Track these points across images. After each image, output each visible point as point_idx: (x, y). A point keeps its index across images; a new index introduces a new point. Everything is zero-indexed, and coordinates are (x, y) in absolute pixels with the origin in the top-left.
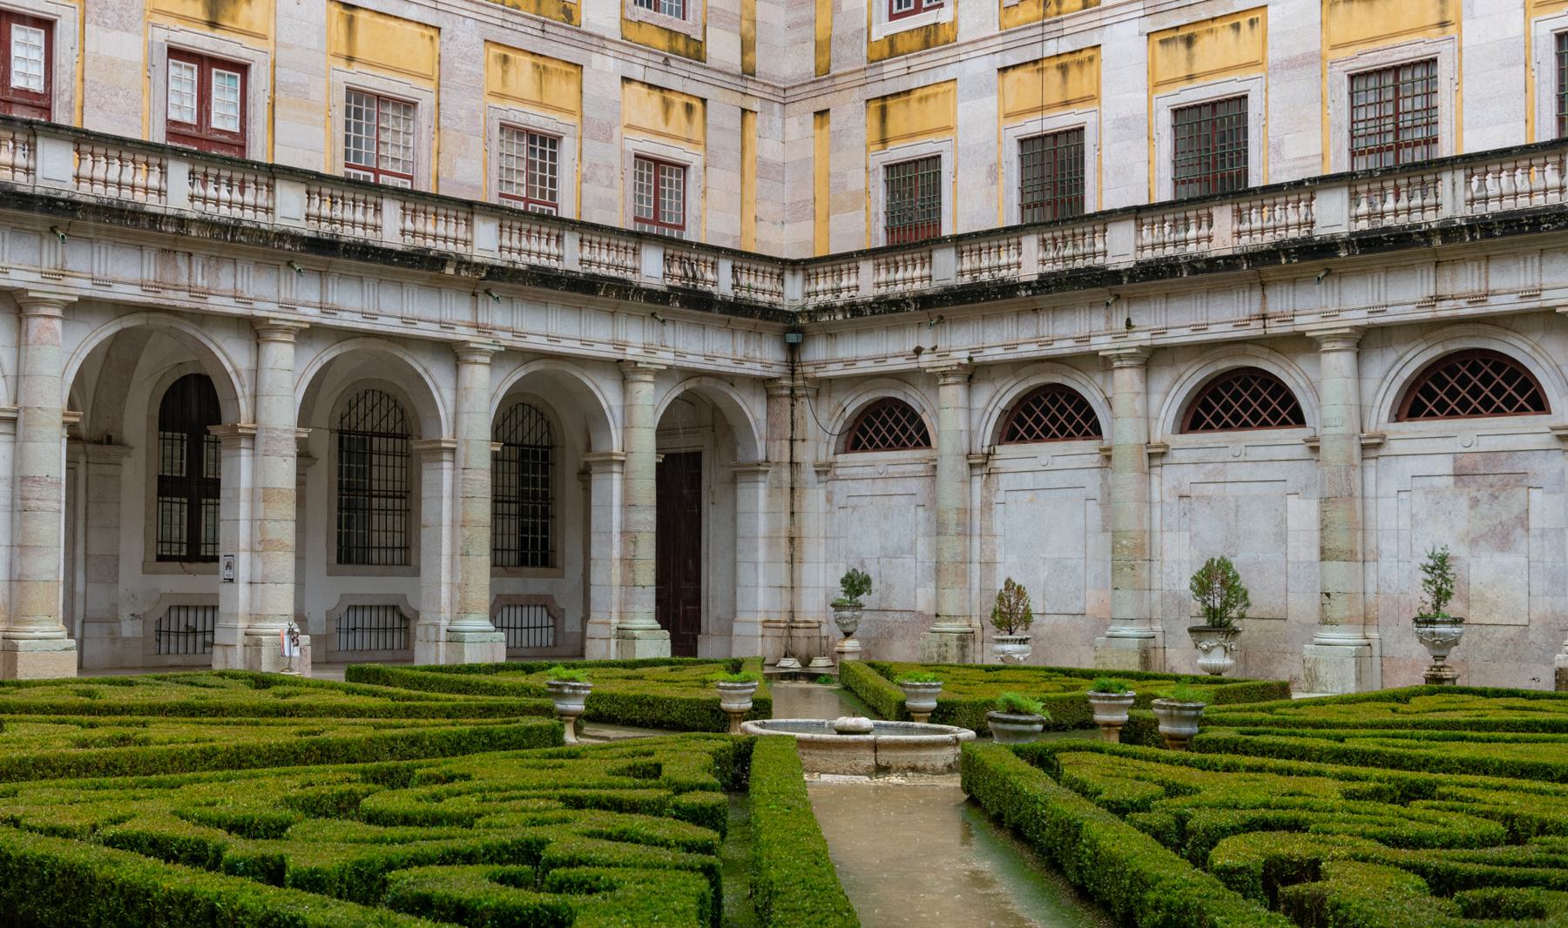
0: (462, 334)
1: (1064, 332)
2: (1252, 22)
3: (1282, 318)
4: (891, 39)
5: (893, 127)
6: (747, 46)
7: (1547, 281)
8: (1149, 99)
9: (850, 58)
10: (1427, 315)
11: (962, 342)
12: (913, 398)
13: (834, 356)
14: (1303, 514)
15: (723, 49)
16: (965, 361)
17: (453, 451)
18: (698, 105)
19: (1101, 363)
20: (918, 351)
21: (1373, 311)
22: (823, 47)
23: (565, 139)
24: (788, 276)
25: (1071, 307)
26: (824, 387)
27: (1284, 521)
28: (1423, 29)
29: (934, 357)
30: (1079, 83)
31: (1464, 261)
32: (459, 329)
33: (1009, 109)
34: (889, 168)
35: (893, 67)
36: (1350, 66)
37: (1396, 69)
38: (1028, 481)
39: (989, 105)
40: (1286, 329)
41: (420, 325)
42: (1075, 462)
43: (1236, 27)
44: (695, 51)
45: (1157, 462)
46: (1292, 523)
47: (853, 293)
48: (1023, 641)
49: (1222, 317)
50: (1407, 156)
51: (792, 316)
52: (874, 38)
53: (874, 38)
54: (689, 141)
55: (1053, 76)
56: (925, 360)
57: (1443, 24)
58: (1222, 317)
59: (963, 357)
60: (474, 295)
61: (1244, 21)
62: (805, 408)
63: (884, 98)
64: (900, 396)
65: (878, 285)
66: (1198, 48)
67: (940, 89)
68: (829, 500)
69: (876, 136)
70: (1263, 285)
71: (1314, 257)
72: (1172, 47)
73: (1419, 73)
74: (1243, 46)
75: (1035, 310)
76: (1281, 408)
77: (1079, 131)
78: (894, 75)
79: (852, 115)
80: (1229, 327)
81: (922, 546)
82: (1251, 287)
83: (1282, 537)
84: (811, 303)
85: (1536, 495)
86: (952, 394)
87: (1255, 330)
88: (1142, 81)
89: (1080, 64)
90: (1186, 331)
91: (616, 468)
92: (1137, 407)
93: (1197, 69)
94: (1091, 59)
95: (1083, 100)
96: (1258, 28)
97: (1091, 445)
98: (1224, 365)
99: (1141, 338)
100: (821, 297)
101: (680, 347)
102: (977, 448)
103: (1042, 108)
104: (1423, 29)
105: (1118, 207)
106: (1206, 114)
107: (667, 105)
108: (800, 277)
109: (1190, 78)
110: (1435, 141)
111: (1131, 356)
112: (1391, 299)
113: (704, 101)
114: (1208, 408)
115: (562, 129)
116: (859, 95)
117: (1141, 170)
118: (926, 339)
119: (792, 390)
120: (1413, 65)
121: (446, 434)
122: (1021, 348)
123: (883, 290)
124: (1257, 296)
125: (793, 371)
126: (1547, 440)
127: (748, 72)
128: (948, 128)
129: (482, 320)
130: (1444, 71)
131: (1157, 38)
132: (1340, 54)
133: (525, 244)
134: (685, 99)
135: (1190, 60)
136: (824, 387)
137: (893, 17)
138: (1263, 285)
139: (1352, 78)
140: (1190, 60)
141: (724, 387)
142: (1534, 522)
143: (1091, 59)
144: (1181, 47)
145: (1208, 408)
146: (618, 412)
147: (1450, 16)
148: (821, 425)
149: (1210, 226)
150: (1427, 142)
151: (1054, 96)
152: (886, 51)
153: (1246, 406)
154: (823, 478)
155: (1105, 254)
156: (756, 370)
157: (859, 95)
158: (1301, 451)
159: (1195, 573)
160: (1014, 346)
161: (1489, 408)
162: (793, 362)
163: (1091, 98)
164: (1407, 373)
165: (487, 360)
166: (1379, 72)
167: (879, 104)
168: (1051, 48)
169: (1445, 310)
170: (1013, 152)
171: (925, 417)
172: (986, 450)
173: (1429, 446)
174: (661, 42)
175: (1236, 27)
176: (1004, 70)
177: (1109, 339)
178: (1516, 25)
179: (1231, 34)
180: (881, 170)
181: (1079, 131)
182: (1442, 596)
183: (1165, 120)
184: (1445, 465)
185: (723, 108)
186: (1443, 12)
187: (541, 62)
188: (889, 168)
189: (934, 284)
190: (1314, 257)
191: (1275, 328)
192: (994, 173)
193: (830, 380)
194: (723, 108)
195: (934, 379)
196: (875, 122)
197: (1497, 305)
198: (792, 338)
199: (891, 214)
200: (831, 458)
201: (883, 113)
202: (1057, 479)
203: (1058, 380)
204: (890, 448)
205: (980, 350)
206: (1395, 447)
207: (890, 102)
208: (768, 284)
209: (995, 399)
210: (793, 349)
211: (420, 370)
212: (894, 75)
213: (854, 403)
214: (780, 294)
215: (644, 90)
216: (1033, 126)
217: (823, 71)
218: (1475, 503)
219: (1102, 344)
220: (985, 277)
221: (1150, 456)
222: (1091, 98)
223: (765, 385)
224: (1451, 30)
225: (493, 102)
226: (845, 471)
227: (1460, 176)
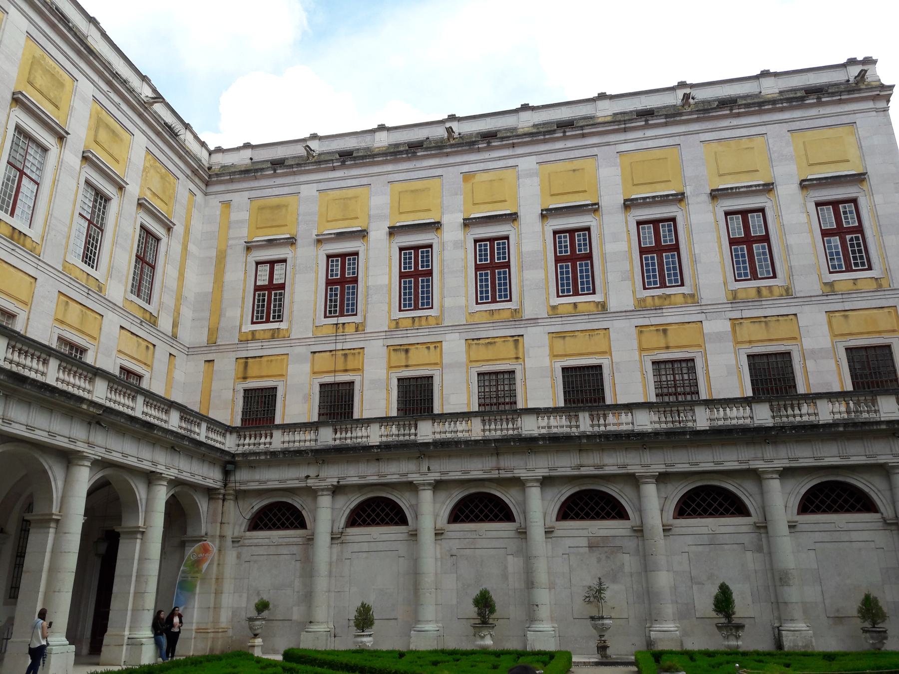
0: (80, 447)
1: (394, 471)
2: (435, 347)
4: (253, 333)
5: (250, 372)
6: (175, 325)
8: (388, 373)
9: (227, 337)
10: (576, 473)
11: (332, 474)
12: (296, 502)
13: (244, 478)
15: (165, 324)
16: (335, 483)
17: (57, 521)
18: (151, 347)
19: (412, 487)
20: (307, 477)
21: (551, 469)
22: (213, 332)
23: (89, 352)
24: (228, 435)
25: (398, 459)
26: (241, 495)
27: (506, 568)
28: (509, 359)
29: (317, 481)
30: (352, 363)
31: (592, 450)
32: (79, 444)
33: (316, 370)
34: (246, 391)
35: (251, 345)
36: (478, 369)
37: (497, 373)
38: (365, 547)
39: (307, 368)
40: (509, 475)
41: (58, 438)
42: (393, 537)
43: (428, 348)
44: (152, 321)
45: (439, 537)
46: (510, 569)
47: (268, 446)
48: (370, 635)
49: (477, 468)
50: (502, 408)
51: (234, 455)
52: (243, 330)
53: (243, 330)
54: (145, 364)
55: (340, 360)
56: (310, 482)
57: (517, 358)
58: (477, 468)
60: (90, 423)
61: (432, 346)
62: (230, 505)
63: (247, 358)
64: (290, 501)
65: (283, 442)
66: (410, 354)
67: (279, 358)
68: (239, 557)
69: (241, 375)
70: (498, 454)
72: (399, 353)
73: (506, 376)
74: (433, 356)
75: (378, 460)
76: (502, 513)
77: (351, 384)
78: (253, 349)
79: (227, 365)
80: (481, 472)
81: (297, 584)
82: (492, 455)
83: (505, 576)
84: (241, 450)
86: (325, 501)
87: (494, 475)
88: (384, 363)
89: (354, 354)
90: (459, 473)
91: (139, 536)
92: (430, 510)
93: (410, 363)
94: (359, 353)
95: (354, 370)
96: (438, 349)
97: (402, 528)
98: (473, 491)
99: (433, 476)
100: (246, 447)
101: (181, 467)
102: (336, 530)
103: (335, 371)
104: (509, 359)
105: (459, 411)
106: (413, 382)
107: (139, 345)
108: (235, 436)
109: (407, 366)
110: (515, 403)
111: (430, 484)
112: (557, 465)
113: (154, 346)
114: (360, 516)
115: (88, 346)
116: (233, 356)
117: (383, 403)
118: (312, 471)
119: (224, 495)
120: (503, 373)
121: (55, 510)
122: (368, 478)
123: (286, 445)
124: (494, 459)
125: (225, 485)
127: (174, 337)
128: (282, 375)
129: (91, 440)
130: (519, 376)
131: (392, 348)
132: (474, 364)
133: (118, 398)
134: (146, 343)
135: (407, 358)
136: (241, 495)
137: (253, 323)
138: (498, 454)
139: (478, 374)
140: (407, 358)
141: (192, 492)
142: (627, 569)
143: (359, 353)
144: (403, 355)
145: (462, 512)
146: (144, 502)
147: (520, 355)
148: (236, 516)
149: (416, 429)
150: (511, 403)
151: (340, 366)
152: (250, 337)
153: (279, 520)
154: (236, 545)
155: (416, 435)
156: (210, 483)
157: (233, 356)
158: (512, 534)
159: (492, 593)
160: (364, 477)
161: (598, 516)
162: (226, 480)
163: (359, 369)
164: (563, 499)
165: (89, 464)
166: (490, 374)
167: (243, 360)
168: (339, 346)
169: (584, 471)
170: (317, 389)
171: (304, 513)
172: (340, 530)
173: (576, 533)
174: (139, 314)
175: (428, 348)
177: (418, 475)
178: (546, 361)
179: (426, 351)
181: (351, 384)
183: (395, 382)
184: (584, 542)
185: (162, 350)
186: (517, 353)
187: (84, 309)
188: (246, 391)
189: (319, 443)
191: (504, 474)
192: (307, 398)
193: (245, 491)
194: (162, 350)
195: (312, 493)
196: (241, 368)
197: (608, 470)
198: (229, 467)
199: (244, 413)
200: (243, 534)
201: (246, 364)
202: (381, 546)
203: (384, 495)
204: (278, 528)
205: (344, 478)
207: (250, 360)
208: (219, 438)
209: (348, 503)
210: (226, 473)
211: (47, 467)
212: (253, 349)
213: (258, 504)
214: (223, 444)
215: (129, 334)
216: (329, 379)
217: (212, 342)
218: (599, 560)
219: (414, 478)
220: (349, 441)
221: (332, 539)
222: (359, 369)
223: (210, 493)
224: (520, 361)
225: (57, 324)
226: (247, 541)
227: (587, 415)
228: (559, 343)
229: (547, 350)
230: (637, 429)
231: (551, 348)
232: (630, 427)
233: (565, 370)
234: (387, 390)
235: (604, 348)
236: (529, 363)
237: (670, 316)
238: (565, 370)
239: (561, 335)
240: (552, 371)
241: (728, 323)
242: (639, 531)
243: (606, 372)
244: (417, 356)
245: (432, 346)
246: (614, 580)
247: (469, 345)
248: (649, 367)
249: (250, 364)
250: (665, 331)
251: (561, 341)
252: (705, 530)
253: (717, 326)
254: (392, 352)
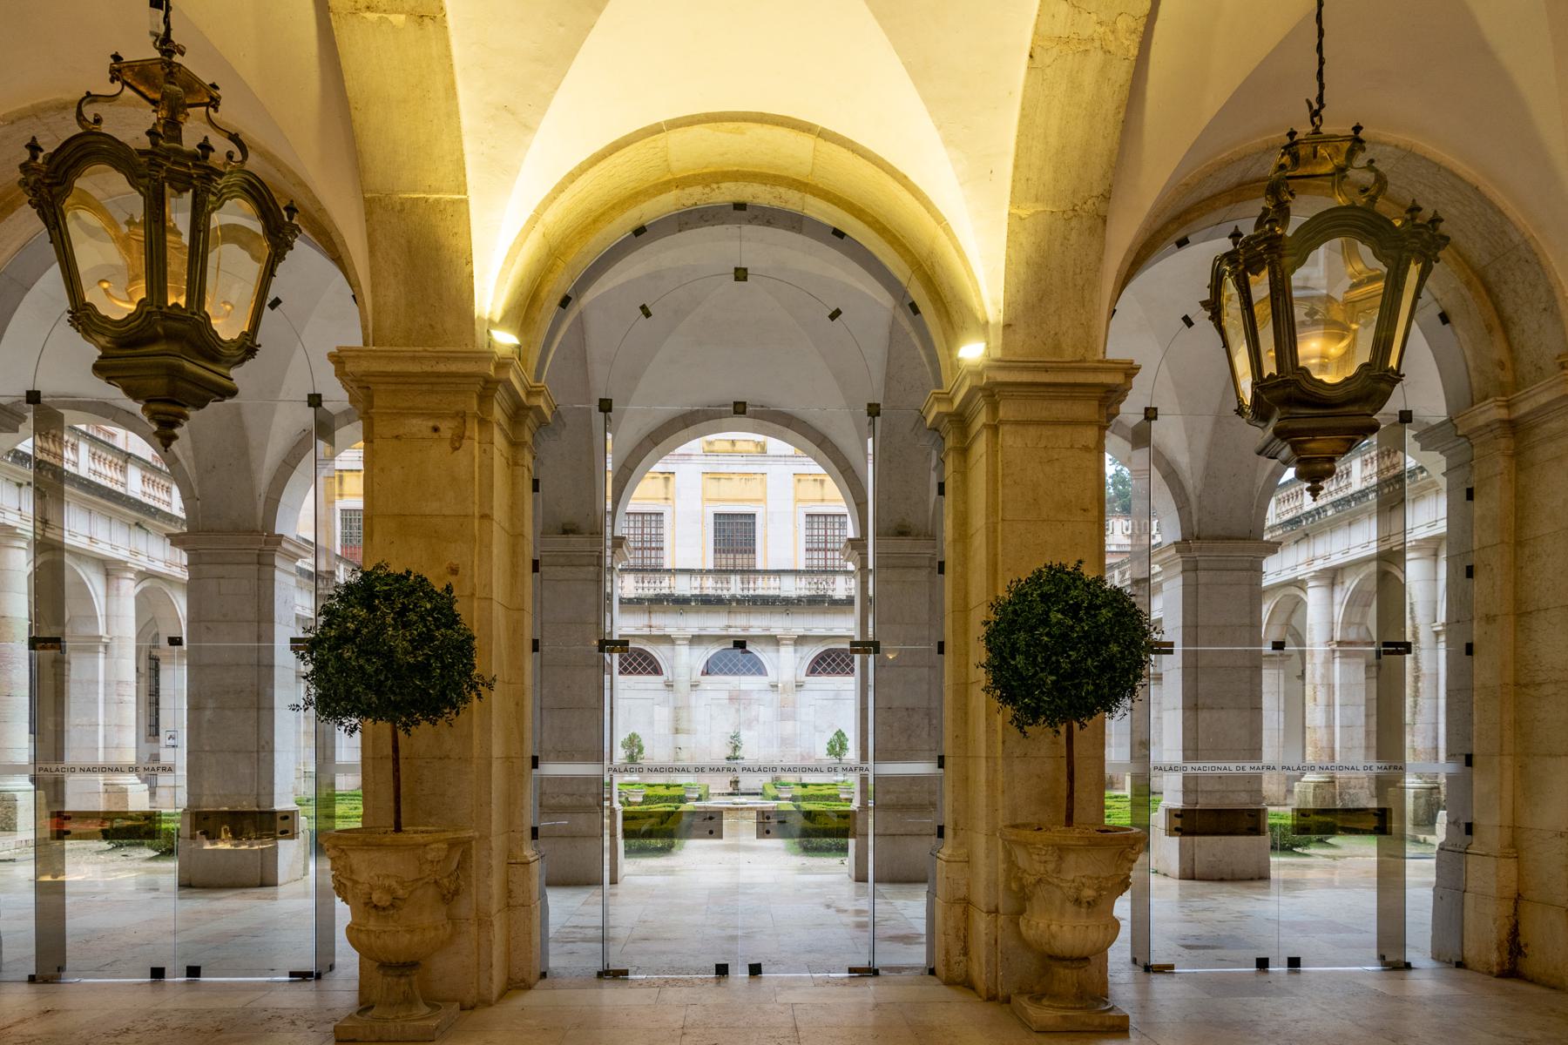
3: (659, 628)
7: (772, 624)
14: (663, 714)
71: (680, 603)
83: (651, 723)
87: (646, 631)
130: (667, 519)
158: (662, 686)
182: (736, 748)
184: (726, 695)
190: (680, 603)
191: (655, 632)
206: (703, 686)
230: (783, 594)
232: (776, 592)
239: (716, 476)
243: (759, 521)
246: (749, 726)
248: (803, 519)
251: (715, 483)
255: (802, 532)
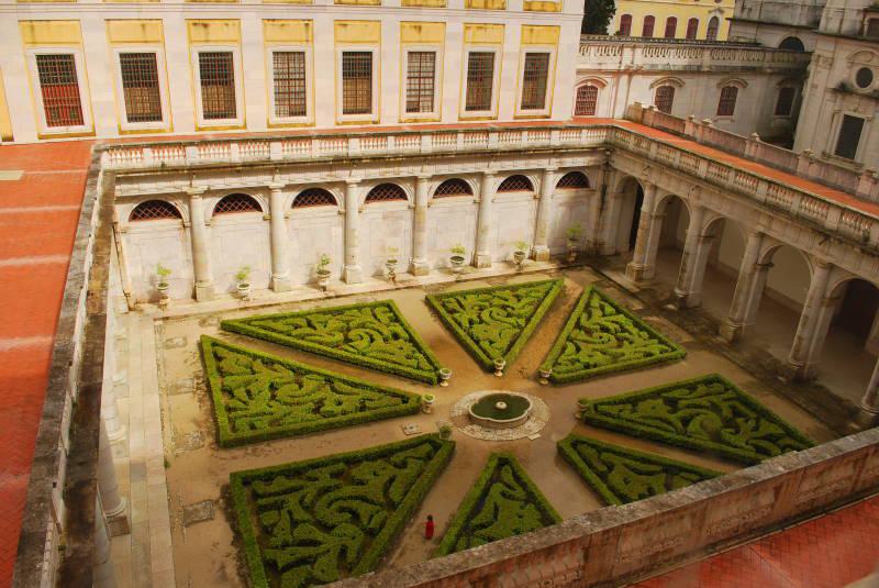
11: (201, 184)
59: (205, 188)
66: (211, 29)
68: (128, 241)
85: (403, 222)
109: (207, 41)
126: (405, 208)
131: (191, 22)
140: (207, 34)
148: (122, 212)
167: (29, 23)
175: (227, 25)
176: (108, 20)
179: (225, 27)
180: (35, 58)
207: (35, 24)
228: (341, 30)
229: (332, 37)
231: (336, 36)
233: (345, 53)
234: (191, 63)
235: (376, 39)
236: (317, 46)
237: (425, 16)
238: (345, 53)
240: (336, 55)
241: (462, 26)
242: (414, 209)
244: (216, 31)
245: (230, 23)
247: (265, 25)
249: (36, 29)
250: (420, 28)
252: (447, 205)
253: (455, 27)
254: (192, 27)
255: (406, 64)
